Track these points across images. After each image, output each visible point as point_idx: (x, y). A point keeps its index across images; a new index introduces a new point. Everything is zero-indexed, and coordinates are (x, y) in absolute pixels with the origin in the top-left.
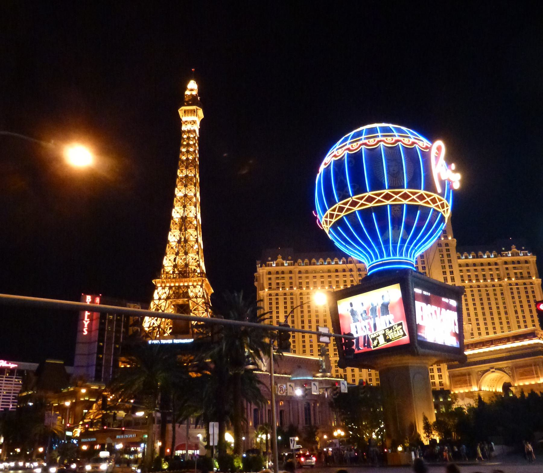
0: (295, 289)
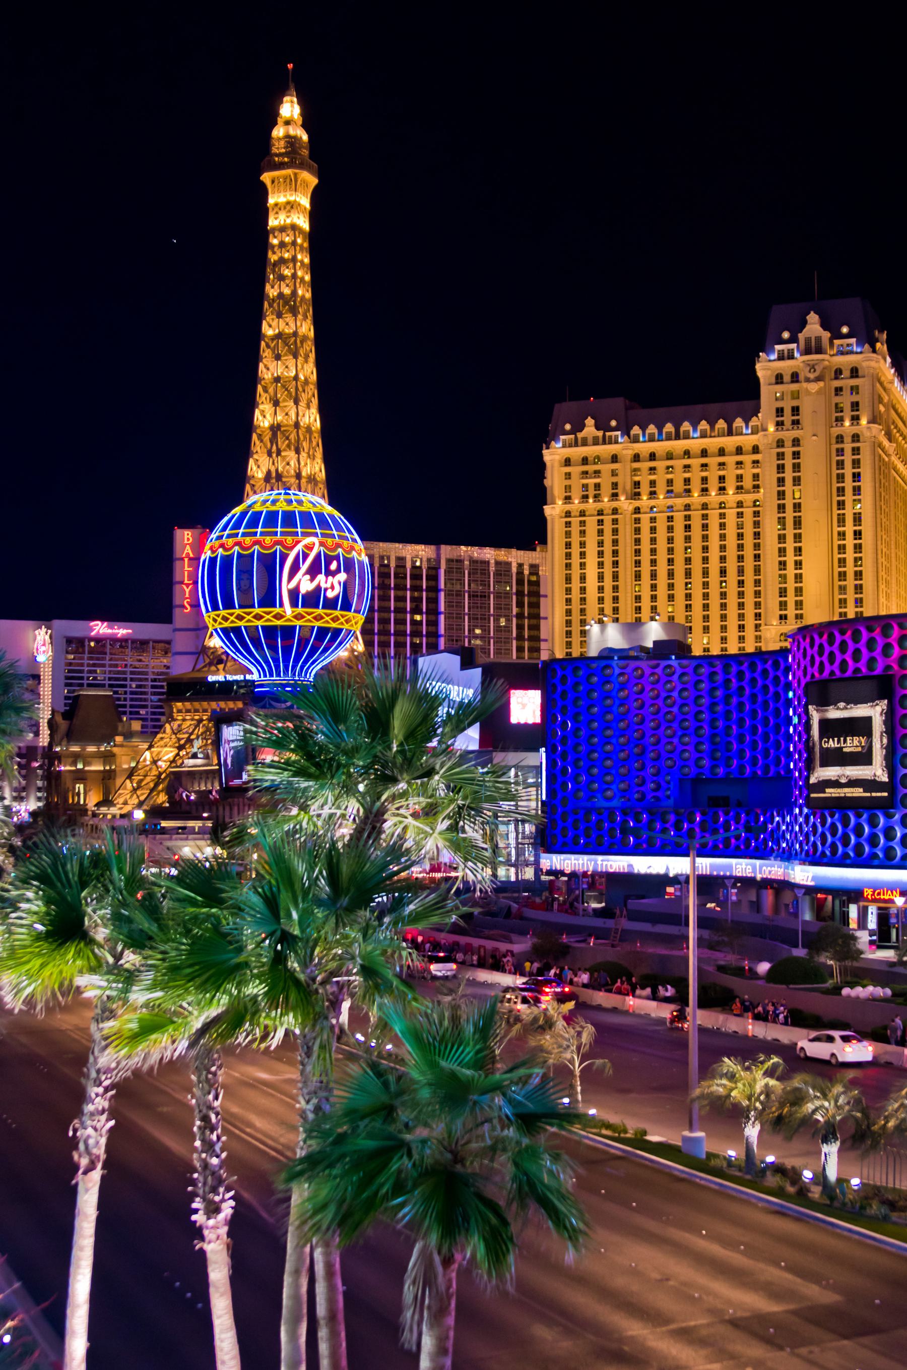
0: (623, 498)
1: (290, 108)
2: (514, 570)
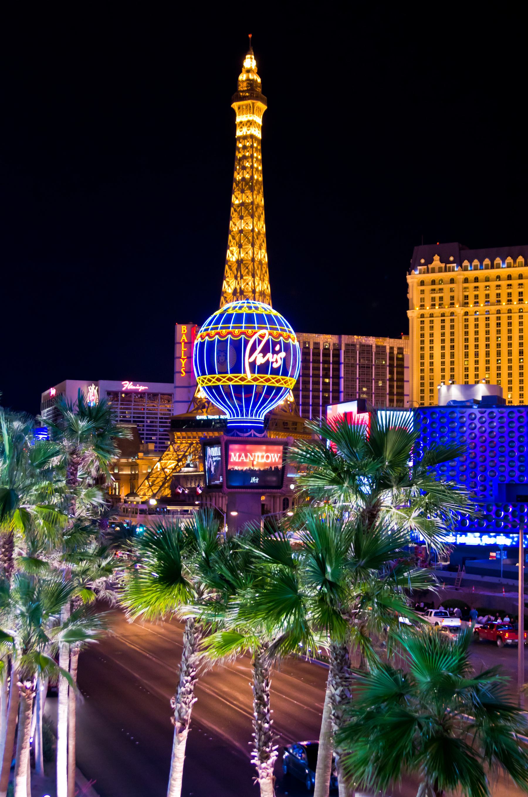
1: (250, 62)
2: (388, 351)
